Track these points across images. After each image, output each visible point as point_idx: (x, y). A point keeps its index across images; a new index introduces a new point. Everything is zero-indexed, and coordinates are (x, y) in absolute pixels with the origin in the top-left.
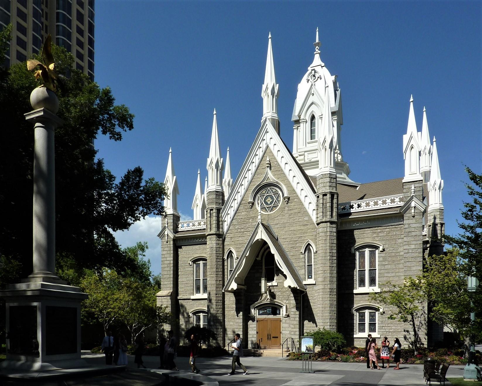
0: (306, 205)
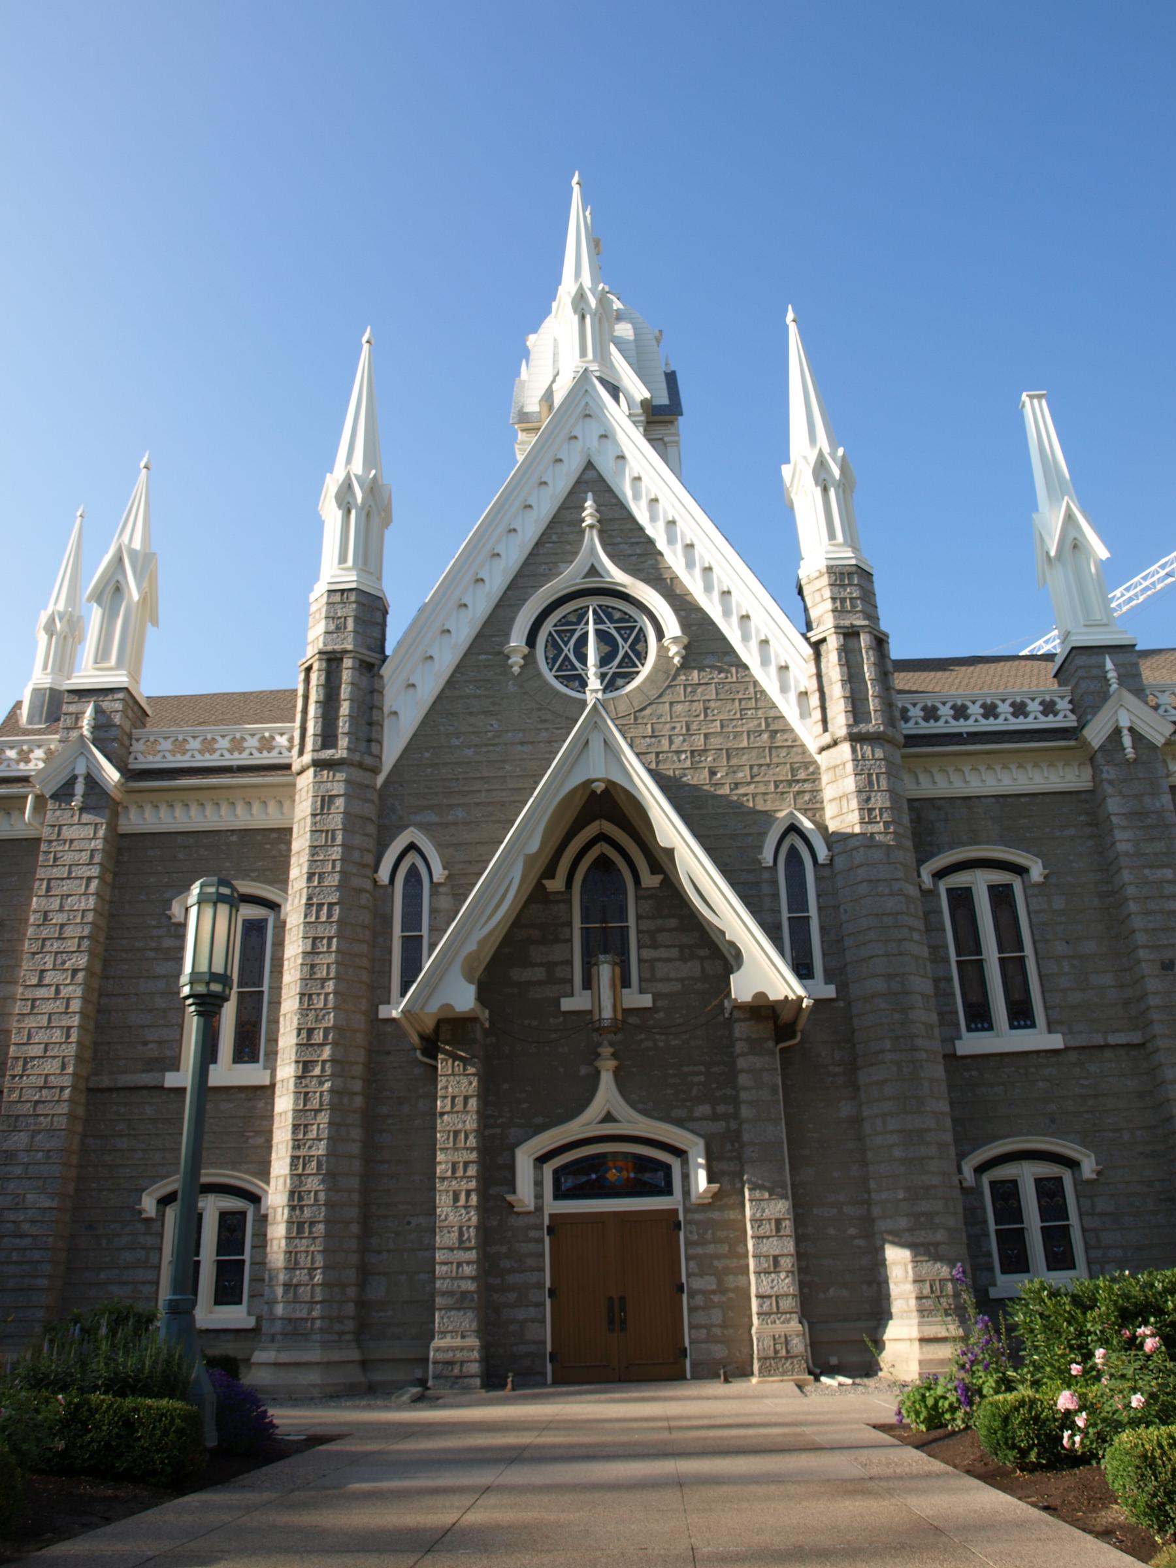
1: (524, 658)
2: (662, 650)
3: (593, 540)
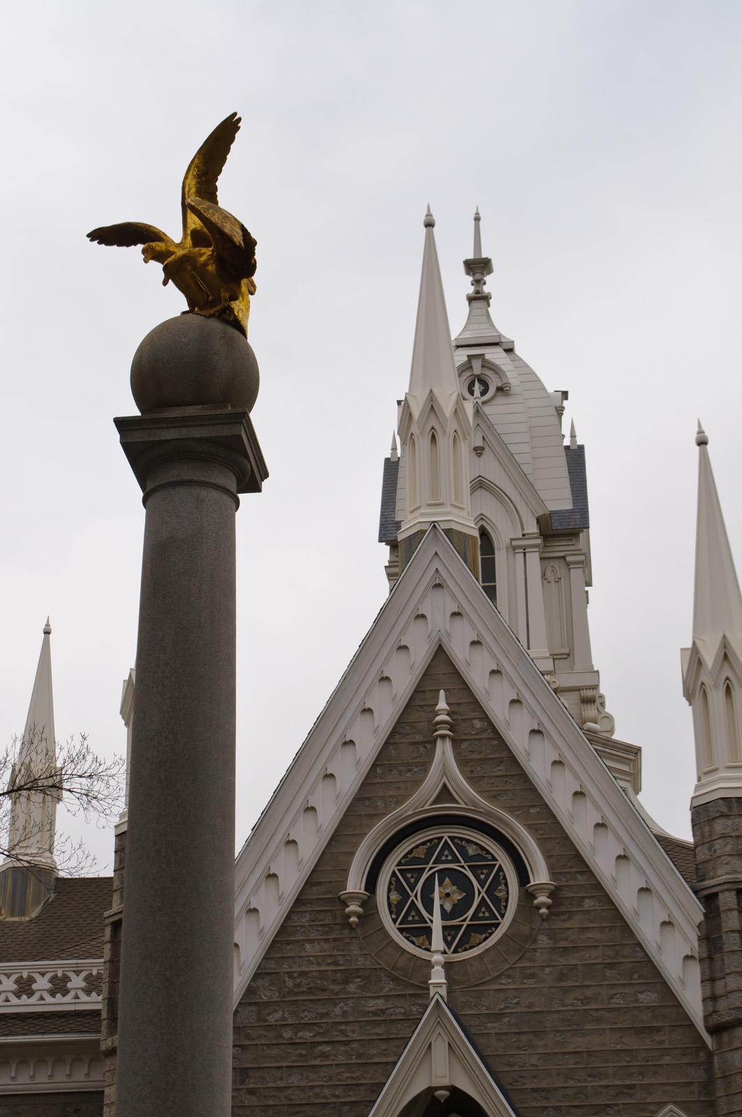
0: (647, 930)
1: (364, 904)
2: (528, 895)
3: (444, 752)
